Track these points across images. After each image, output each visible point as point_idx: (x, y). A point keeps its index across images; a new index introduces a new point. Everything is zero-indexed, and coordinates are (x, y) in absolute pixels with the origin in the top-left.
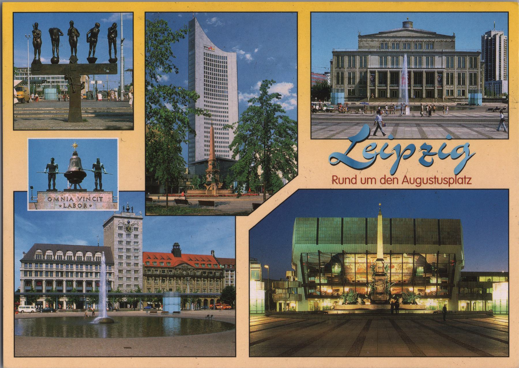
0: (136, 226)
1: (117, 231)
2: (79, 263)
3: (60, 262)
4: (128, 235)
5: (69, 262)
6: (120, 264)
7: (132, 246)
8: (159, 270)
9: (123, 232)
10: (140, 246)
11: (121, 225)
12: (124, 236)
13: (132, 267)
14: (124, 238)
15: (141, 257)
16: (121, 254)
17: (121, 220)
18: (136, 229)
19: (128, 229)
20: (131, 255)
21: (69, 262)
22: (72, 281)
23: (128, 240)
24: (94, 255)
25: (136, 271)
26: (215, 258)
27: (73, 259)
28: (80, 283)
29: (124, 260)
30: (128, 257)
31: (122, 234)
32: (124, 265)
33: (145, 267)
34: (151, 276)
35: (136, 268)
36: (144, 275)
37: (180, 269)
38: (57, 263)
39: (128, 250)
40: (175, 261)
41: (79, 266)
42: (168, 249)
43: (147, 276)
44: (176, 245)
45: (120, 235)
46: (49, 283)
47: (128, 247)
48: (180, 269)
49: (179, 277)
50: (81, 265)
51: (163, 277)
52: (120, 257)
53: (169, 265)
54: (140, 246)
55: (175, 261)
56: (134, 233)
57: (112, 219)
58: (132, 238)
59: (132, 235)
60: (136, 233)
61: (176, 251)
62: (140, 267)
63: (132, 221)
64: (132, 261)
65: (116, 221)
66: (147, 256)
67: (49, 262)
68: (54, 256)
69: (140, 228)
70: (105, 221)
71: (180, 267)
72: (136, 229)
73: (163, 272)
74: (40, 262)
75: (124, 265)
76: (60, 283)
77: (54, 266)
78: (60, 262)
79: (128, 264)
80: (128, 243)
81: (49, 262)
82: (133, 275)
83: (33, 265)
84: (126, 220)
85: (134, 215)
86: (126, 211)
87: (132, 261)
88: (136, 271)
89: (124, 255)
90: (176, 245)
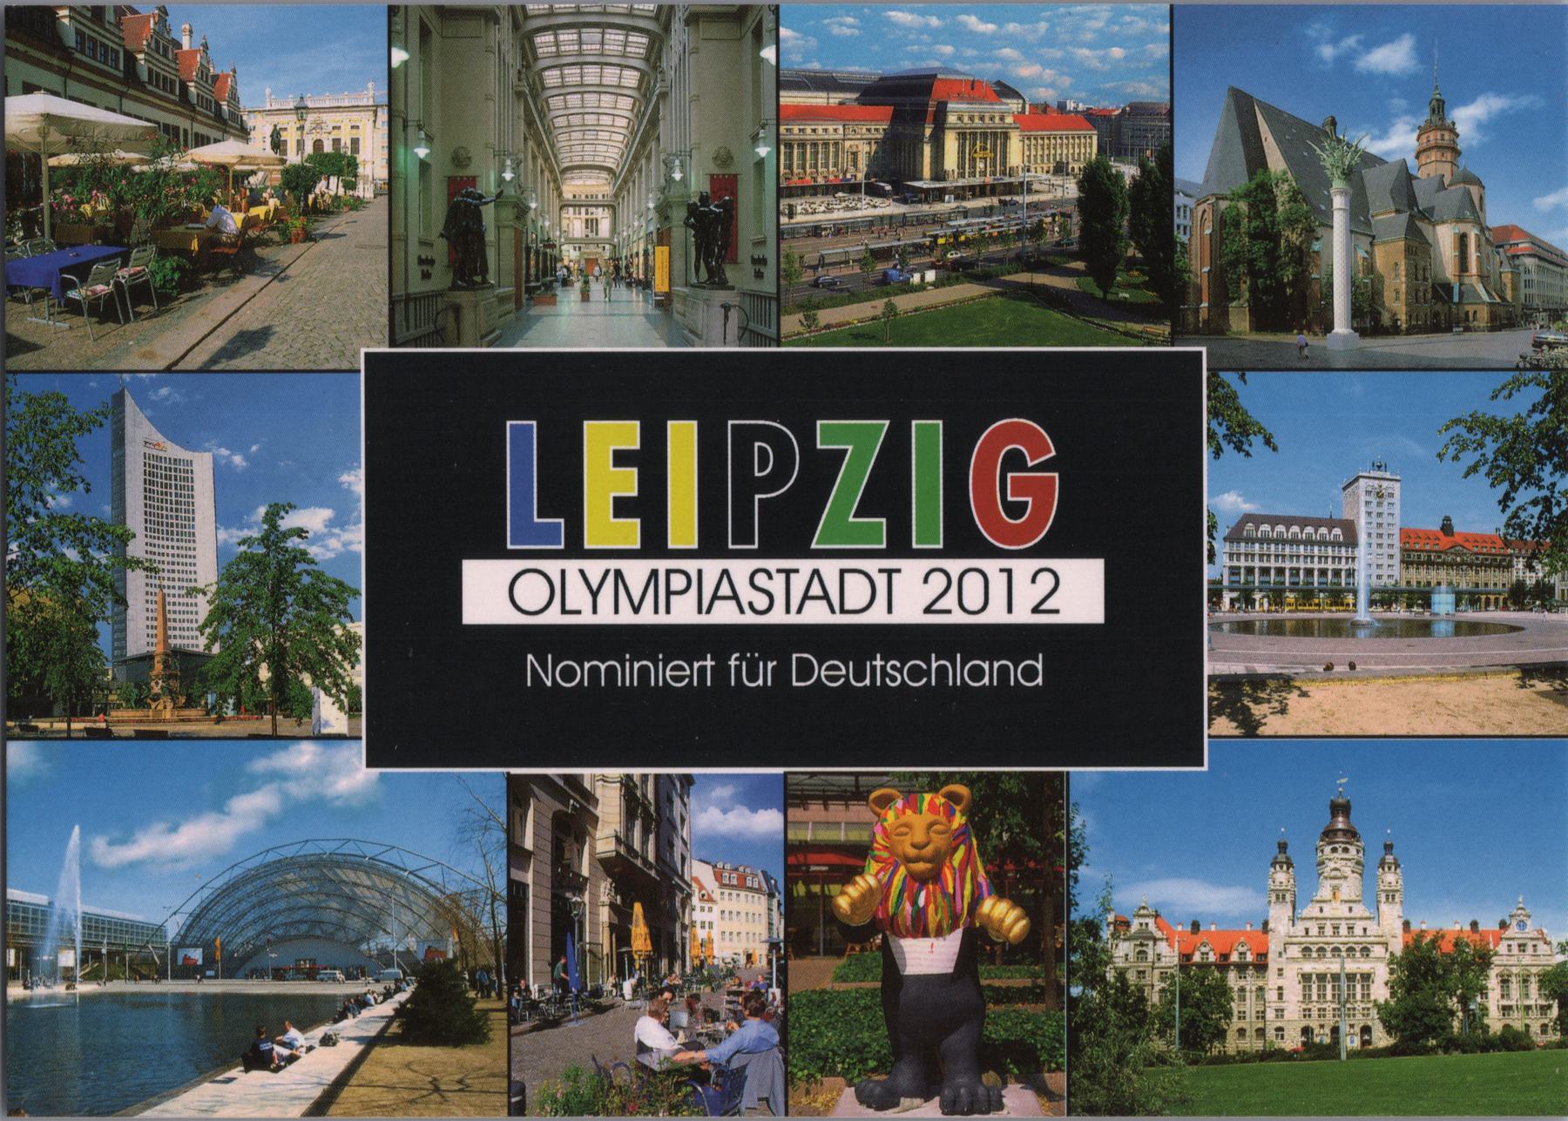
1: (1363, 498)
3: (1280, 541)
14: (1374, 509)
15: (1397, 538)
17: (1371, 482)
19: (1380, 495)
21: (1295, 542)
22: (1298, 570)
25: (1391, 556)
28: (1309, 572)
33: (1403, 550)
34: (1412, 563)
35: (1391, 552)
36: (1402, 561)
38: (1277, 542)
40: (1445, 542)
42: (1435, 526)
44: (1447, 519)
46: (1265, 571)
49: (1451, 565)
51: (1429, 563)
55: (1445, 542)
57: (1357, 479)
58: (1385, 509)
61: (1447, 528)
62: (1396, 551)
63: (1385, 484)
65: (1362, 482)
66: (1406, 535)
69: (1397, 493)
70: (1345, 482)
72: (1391, 495)
74: (1251, 541)
76: (1280, 571)
78: (1280, 541)
82: (1385, 561)
85: (1388, 475)
90: (1447, 519)
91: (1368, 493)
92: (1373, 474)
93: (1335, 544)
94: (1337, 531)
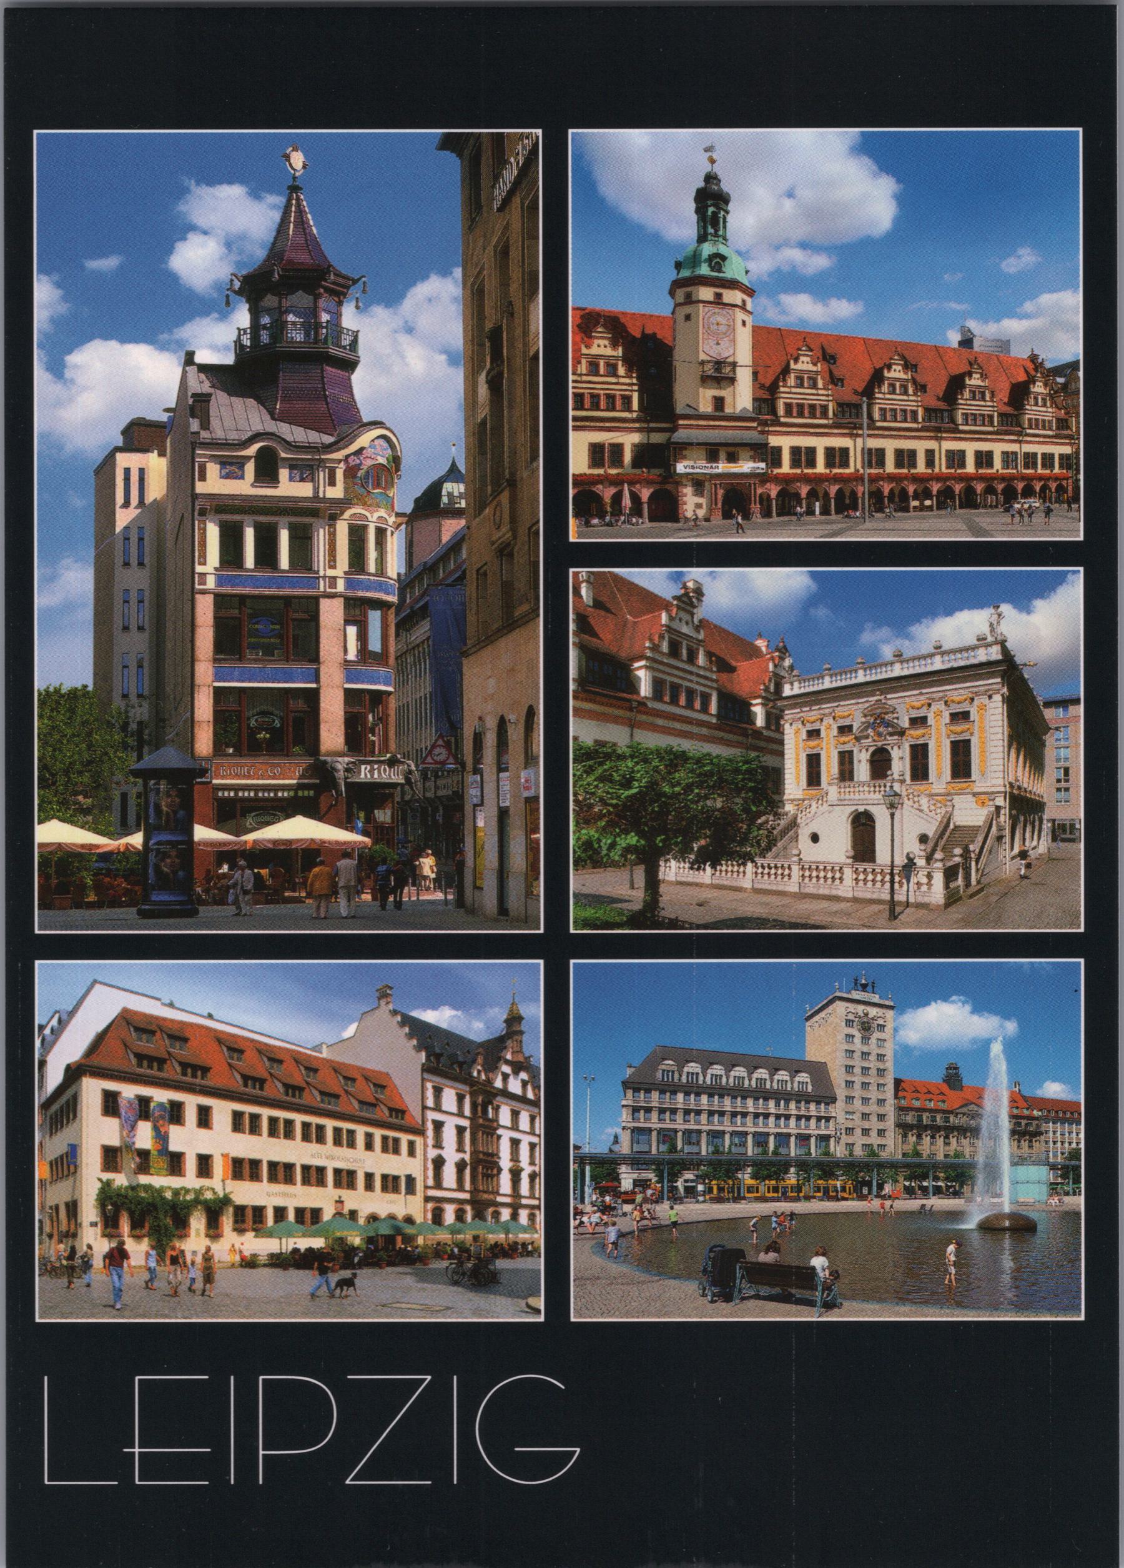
0: (881, 1022)
2: (761, 1094)
3: (716, 1090)
4: (865, 1039)
5: (739, 1092)
6: (849, 1099)
7: (873, 1063)
8: (912, 1113)
9: (854, 1031)
10: (889, 1064)
11: (851, 1017)
12: (857, 1040)
13: (873, 1108)
15: (890, 1087)
16: (849, 1079)
17: (852, 1007)
18: (881, 1027)
19: (866, 1027)
20: (872, 1081)
23: (865, 1049)
24: (750, 1074)
26: (1023, 1097)
27: (768, 1086)
29: (857, 1092)
30: (865, 1085)
31: (853, 1036)
32: (857, 1103)
33: (900, 1109)
35: (881, 1111)
36: (899, 1125)
37: (964, 1114)
39: (865, 1070)
41: (761, 1101)
43: (903, 1128)
45: (850, 1037)
47: (866, 1064)
48: (964, 1114)
50: (766, 1099)
52: (849, 1084)
53: (941, 1105)
54: (889, 1064)
56: (877, 1035)
58: (873, 1047)
59: (873, 1040)
60: (882, 1036)
62: (890, 1109)
63: (873, 1012)
64: (873, 1094)
67: (693, 1089)
68: (750, 1080)
71: (964, 1110)
72: (881, 1027)
73: (934, 1119)
74: (669, 1088)
75: (857, 1103)
77: (704, 1099)
78: (716, 1090)
79: (865, 1100)
80: (865, 1055)
81: (693, 1089)
82: (874, 1124)
83: (655, 1095)
84: (860, 1008)
85: (876, 999)
86: (860, 988)
87: (873, 1094)
88: (881, 1117)
89: (858, 1079)
91: (849, 1023)
92: (856, 995)
93: (802, 1097)
94: (803, 1077)
